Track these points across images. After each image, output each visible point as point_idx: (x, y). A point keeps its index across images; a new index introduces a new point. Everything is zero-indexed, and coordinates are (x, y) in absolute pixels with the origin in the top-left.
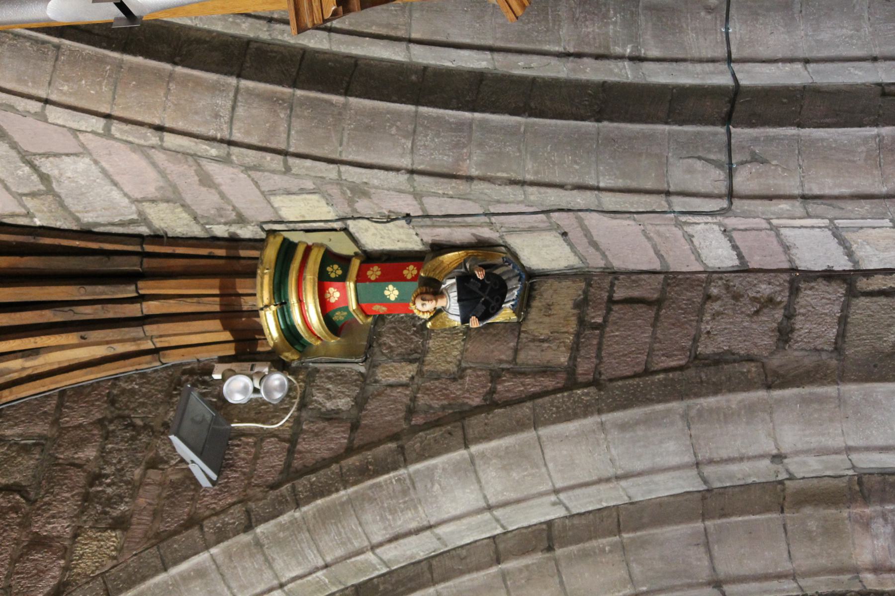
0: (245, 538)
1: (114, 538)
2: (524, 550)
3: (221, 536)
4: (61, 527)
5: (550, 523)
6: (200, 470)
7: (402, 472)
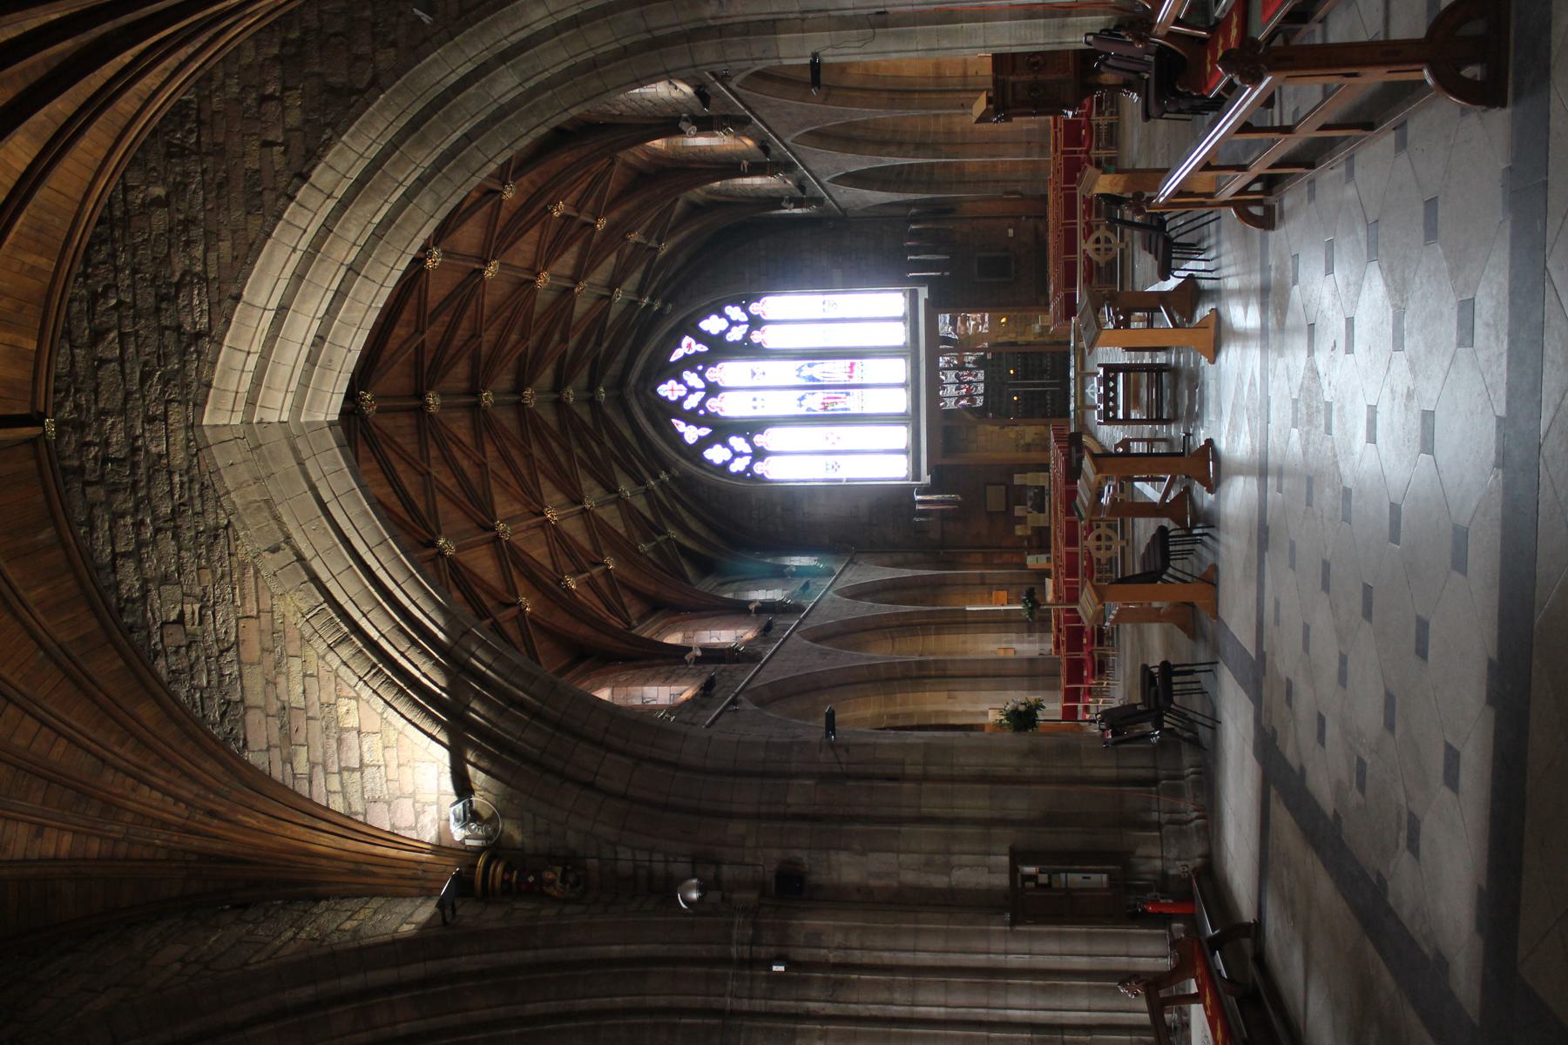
0: (451, 43)
1: (392, 52)
2: (568, 29)
3: (440, 44)
4: (366, 49)
5: (575, 15)
6: (426, 19)
7: (512, 6)
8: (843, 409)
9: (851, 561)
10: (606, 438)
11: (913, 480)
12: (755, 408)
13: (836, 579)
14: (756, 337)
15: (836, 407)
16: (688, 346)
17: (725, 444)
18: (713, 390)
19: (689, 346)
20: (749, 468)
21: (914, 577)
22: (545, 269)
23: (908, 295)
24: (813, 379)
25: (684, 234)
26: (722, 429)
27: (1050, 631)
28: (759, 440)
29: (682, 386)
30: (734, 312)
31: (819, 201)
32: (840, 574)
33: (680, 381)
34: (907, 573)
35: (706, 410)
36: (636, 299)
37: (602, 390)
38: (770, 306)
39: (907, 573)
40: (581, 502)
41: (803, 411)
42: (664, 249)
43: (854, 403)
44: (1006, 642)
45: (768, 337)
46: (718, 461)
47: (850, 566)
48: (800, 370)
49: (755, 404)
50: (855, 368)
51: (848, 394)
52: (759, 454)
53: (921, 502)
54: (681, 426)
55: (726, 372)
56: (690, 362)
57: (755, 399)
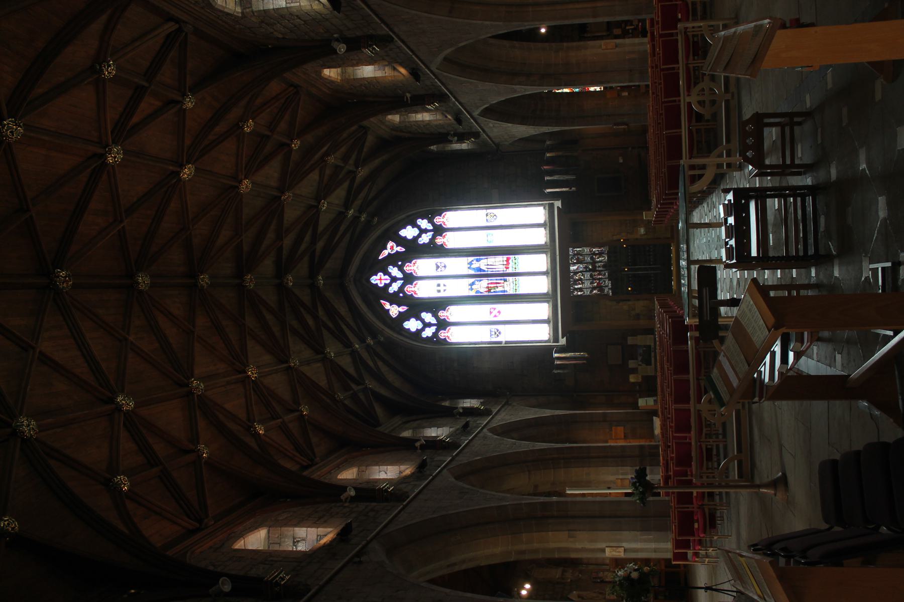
8: (502, 291)
9: (507, 403)
10: (321, 313)
11: (553, 342)
12: (439, 291)
13: (492, 418)
14: (439, 240)
15: (497, 290)
16: (392, 248)
17: (419, 318)
18: (409, 278)
19: (392, 248)
20: (435, 334)
21: (552, 416)
22: (246, 178)
23: (547, 208)
24: (480, 270)
25: (377, 162)
26: (416, 307)
27: (658, 465)
28: (442, 314)
29: (387, 277)
30: (424, 223)
31: (476, 135)
32: (496, 414)
33: (387, 273)
34: (547, 413)
35: (404, 293)
36: (344, 211)
37: (320, 278)
38: (451, 218)
39: (547, 413)
40: (287, 362)
41: (473, 293)
42: (362, 173)
43: (509, 287)
44: (622, 474)
45: (450, 241)
46: (413, 329)
47: (506, 407)
48: (471, 263)
49: (439, 288)
50: (510, 261)
51: (505, 280)
52: (443, 324)
53: (558, 358)
54: (387, 306)
55: (422, 266)
56: (393, 259)
57: (439, 285)
